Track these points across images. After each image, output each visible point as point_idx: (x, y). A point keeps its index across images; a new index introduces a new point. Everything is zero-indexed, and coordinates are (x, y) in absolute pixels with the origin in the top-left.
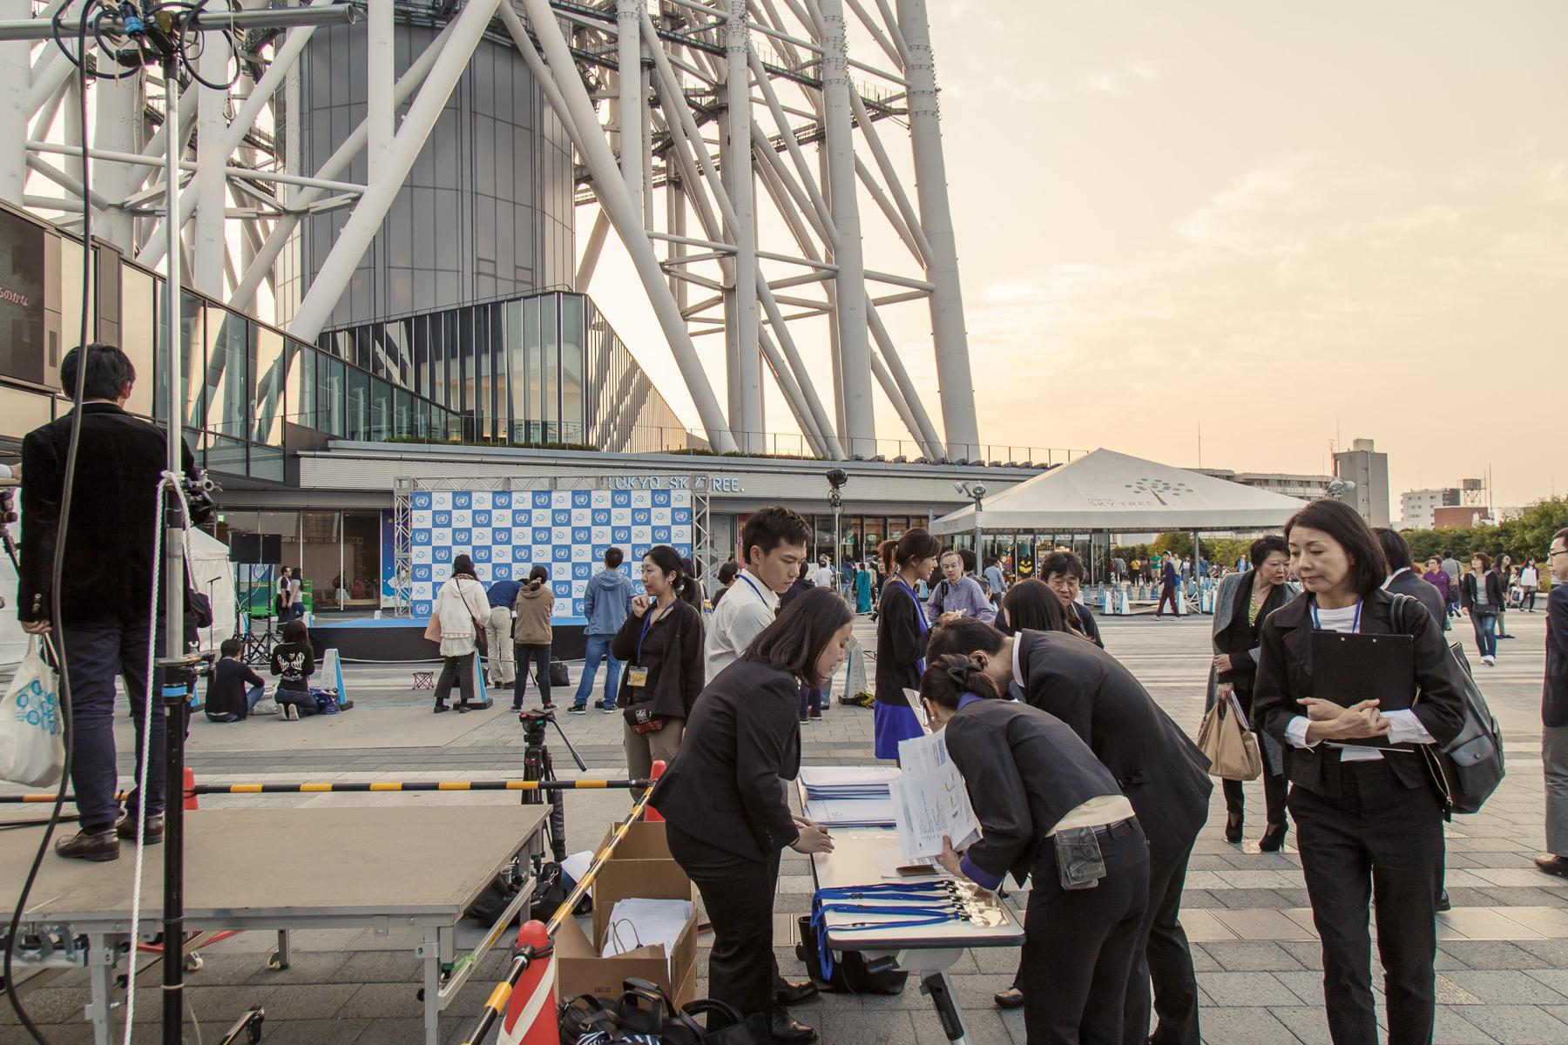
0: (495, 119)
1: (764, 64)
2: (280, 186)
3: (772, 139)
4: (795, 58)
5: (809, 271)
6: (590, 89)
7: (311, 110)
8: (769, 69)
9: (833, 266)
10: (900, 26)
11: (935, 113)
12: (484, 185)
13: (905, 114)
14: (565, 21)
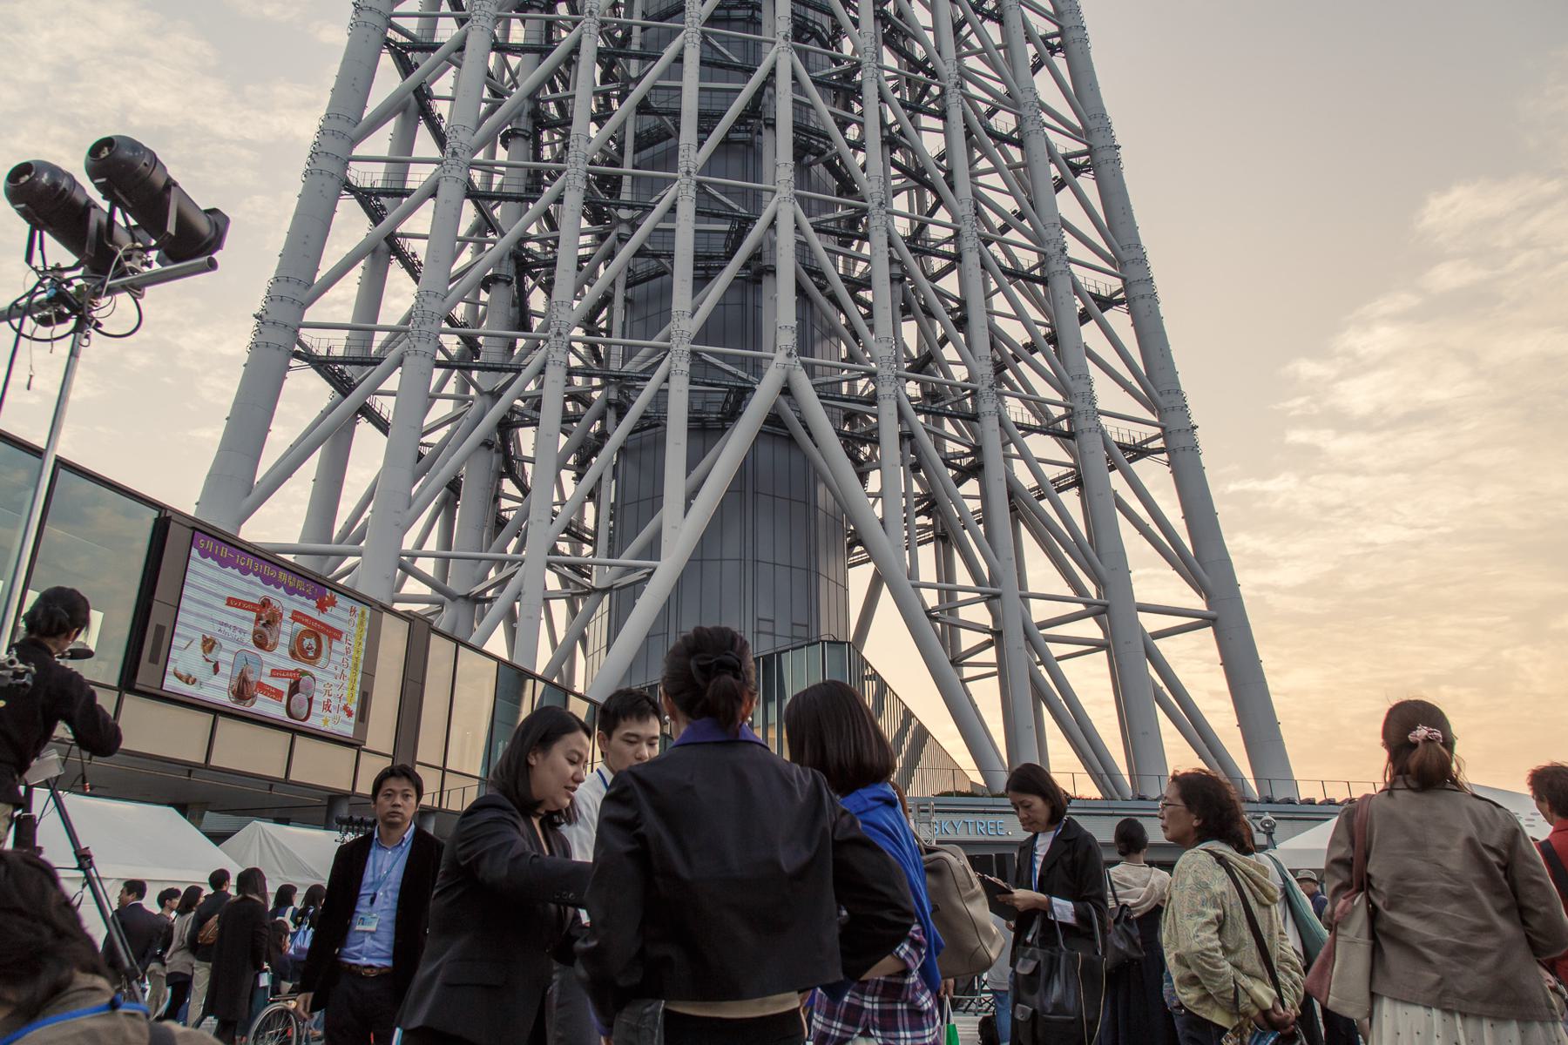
0: (774, 496)
1: (1016, 423)
2: (595, 567)
3: (1031, 490)
4: (1047, 414)
5: (1080, 607)
6: (857, 462)
7: (623, 505)
8: (1020, 426)
9: (1103, 601)
10: (1147, 376)
11: (1194, 449)
12: (764, 552)
13: (1163, 452)
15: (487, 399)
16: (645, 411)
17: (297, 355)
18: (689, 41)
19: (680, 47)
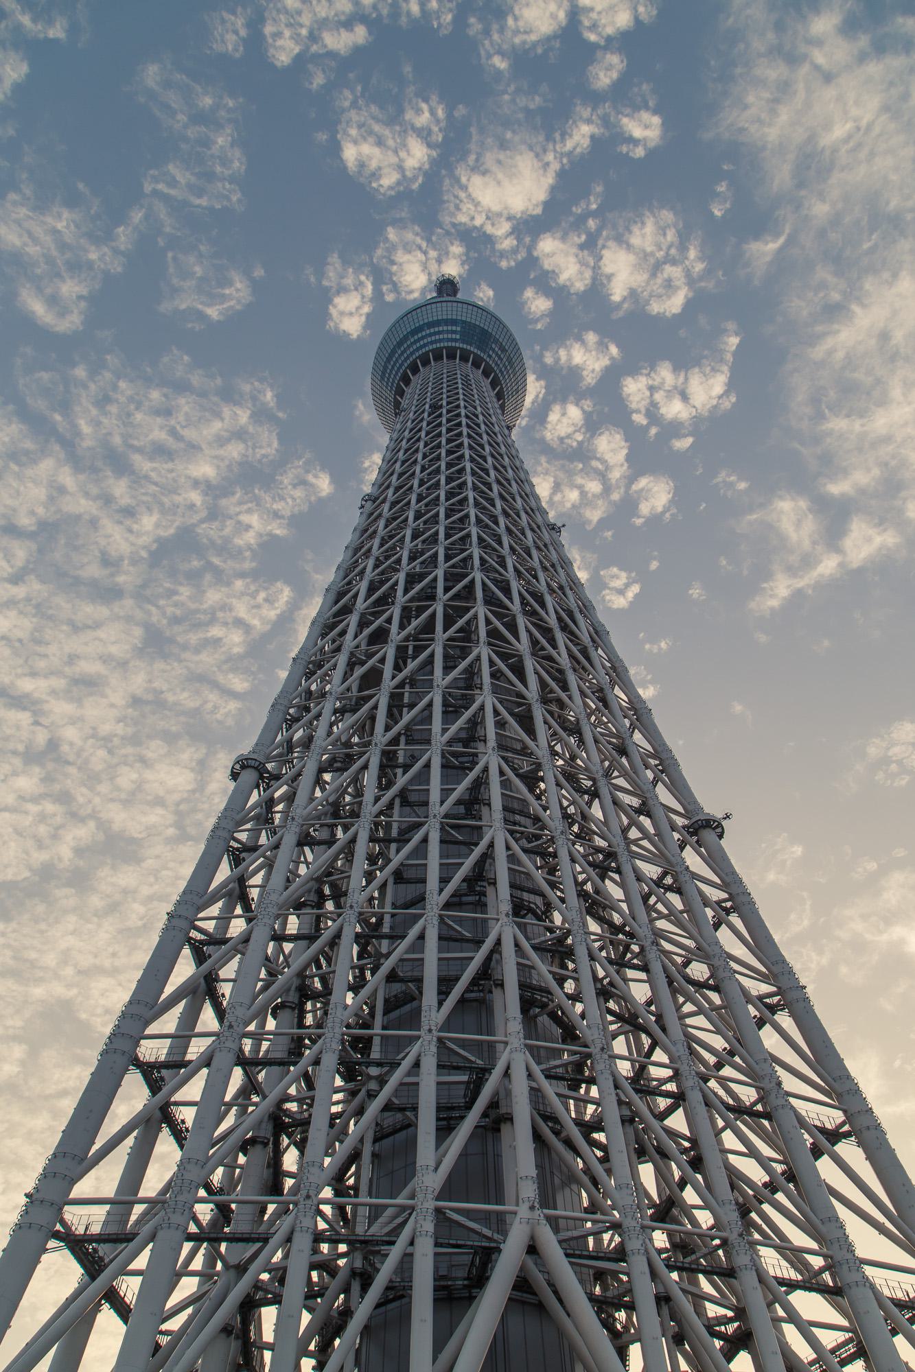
4: (807, 1265)
6: (615, 1335)
8: (782, 1282)
10: (899, 1216)
14: (585, 1270)
15: (232, 1273)
16: (391, 1281)
17: (56, 1235)
18: (429, 922)
19: (421, 928)
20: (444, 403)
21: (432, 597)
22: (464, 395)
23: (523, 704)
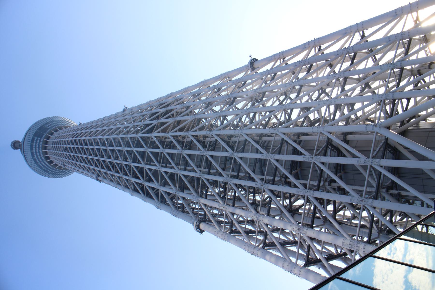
20: (65, 146)
21: (144, 153)
22: (63, 138)
23: (195, 122)
